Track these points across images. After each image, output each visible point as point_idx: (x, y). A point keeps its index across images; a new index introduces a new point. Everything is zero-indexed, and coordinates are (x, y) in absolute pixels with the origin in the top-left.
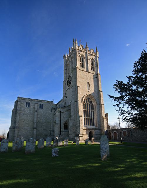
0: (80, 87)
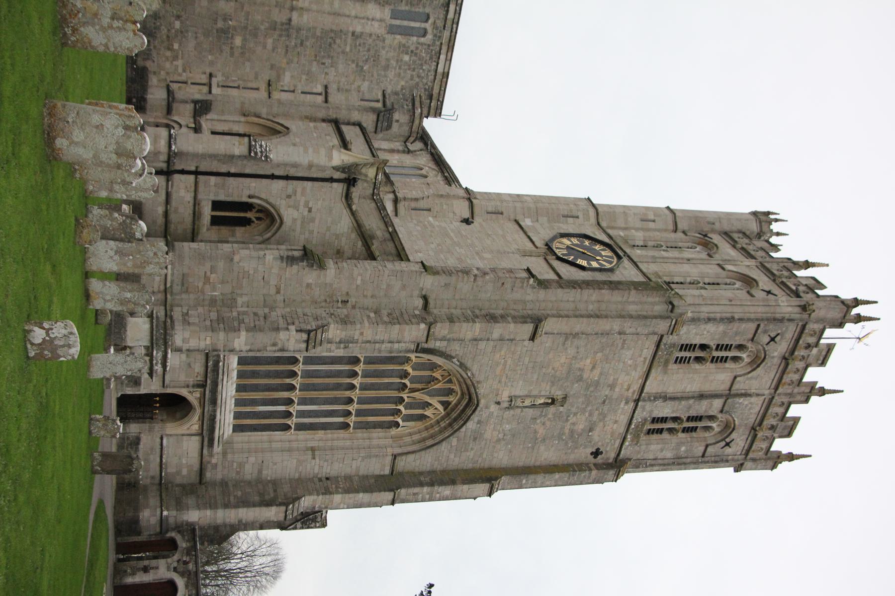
0: (533, 338)
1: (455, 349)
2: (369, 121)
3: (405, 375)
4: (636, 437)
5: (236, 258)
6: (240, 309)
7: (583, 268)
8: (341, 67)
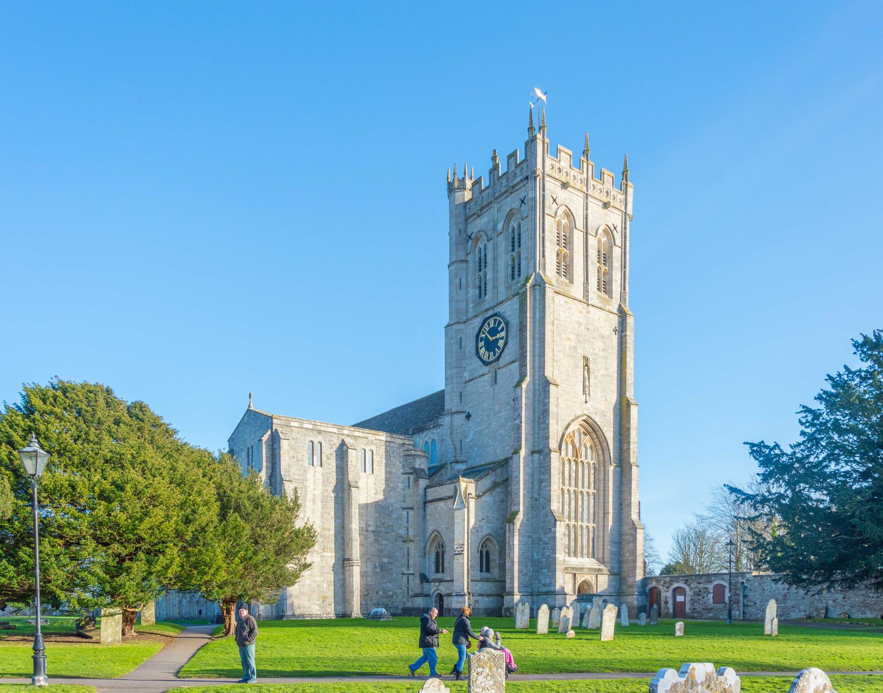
8: (393, 500)
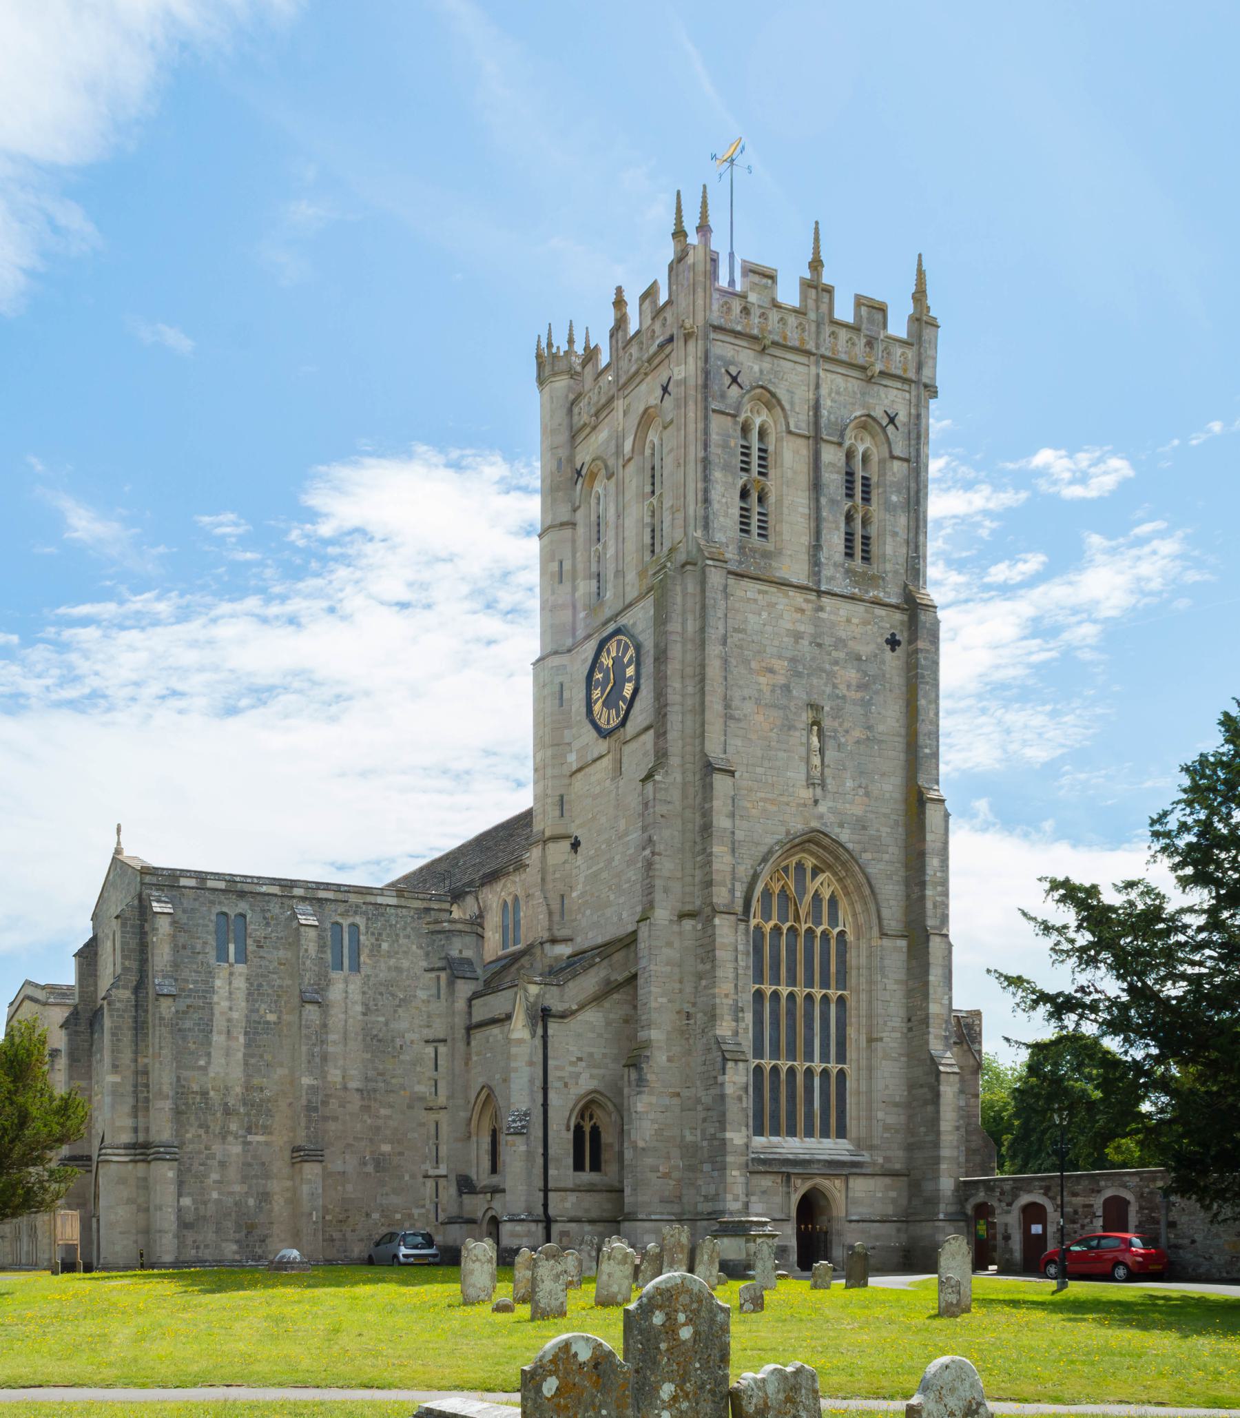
1: (744, 871)
2: (464, 989)
3: (777, 930)
4: (873, 581)
5: (641, 1144)
6: (699, 1138)
7: (636, 691)
8: (404, 1025)
